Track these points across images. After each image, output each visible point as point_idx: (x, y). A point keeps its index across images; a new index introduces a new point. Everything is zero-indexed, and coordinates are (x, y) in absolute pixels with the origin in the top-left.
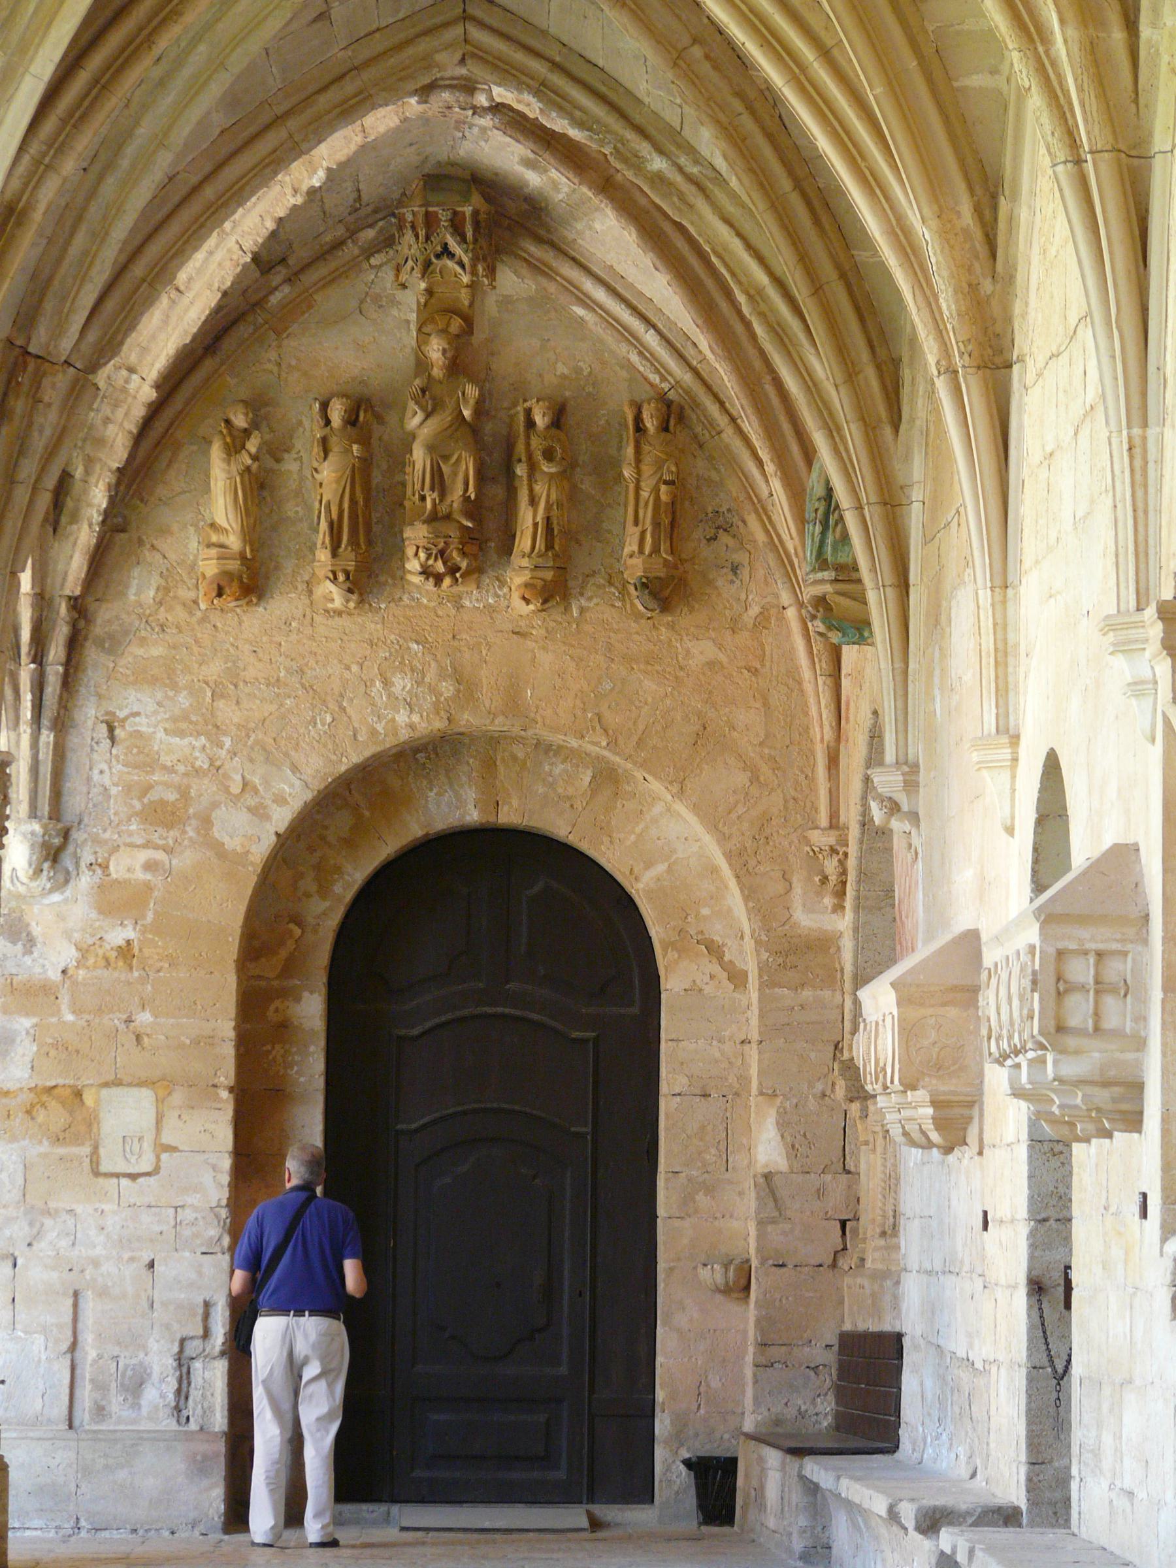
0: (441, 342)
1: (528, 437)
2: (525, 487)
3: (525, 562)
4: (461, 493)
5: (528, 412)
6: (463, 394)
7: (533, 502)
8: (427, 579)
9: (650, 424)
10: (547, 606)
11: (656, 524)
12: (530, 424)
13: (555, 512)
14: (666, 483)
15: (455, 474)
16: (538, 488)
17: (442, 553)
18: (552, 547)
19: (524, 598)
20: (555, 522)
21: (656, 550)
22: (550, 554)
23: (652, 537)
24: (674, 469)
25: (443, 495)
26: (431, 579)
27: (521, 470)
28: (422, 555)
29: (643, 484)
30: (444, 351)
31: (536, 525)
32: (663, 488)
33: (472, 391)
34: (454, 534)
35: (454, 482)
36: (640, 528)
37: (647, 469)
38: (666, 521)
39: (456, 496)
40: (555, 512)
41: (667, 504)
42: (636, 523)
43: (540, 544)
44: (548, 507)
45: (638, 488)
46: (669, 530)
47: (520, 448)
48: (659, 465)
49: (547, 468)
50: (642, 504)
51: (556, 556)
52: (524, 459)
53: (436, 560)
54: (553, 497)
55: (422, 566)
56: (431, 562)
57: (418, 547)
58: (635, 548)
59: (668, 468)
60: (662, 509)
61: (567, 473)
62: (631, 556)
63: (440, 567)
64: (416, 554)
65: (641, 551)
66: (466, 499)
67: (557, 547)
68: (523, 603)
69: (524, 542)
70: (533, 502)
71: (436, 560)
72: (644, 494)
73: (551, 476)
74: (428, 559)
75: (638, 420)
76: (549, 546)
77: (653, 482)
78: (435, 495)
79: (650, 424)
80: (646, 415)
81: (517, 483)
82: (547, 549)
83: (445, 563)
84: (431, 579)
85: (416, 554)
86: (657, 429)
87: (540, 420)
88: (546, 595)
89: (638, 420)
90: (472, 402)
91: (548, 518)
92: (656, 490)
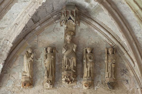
3: (85, 79)
5: (86, 50)
7: (87, 67)
9: (110, 52)
10: (90, 87)
11: (111, 71)
12: (87, 52)
13: (91, 69)
14: (113, 63)
16: (88, 64)
18: (91, 76)
19: (85, 86)
20: (91, 71)
21: (111, 77)
22: (90, 77)
23: (111, 74)
24: (115, 61)
27: (85, 61)
29: (109, 64)
31: (88, 71)
32: (113, 64)
36: (108, 72)
37: (109, 61)
38: (113, 71)
40: (91, 69)
41: (114, 68)
42: (107, 71)
43: (89, 75)
44: (90, 68)
45: (108, 64)
46: (114, 73)
47: (85, 57)
48: (112, 60)
49: (90, 60)
50: (109, 67)
51: (92, 78)
54: (91, 66)
58: (107, 76)
59: (114, 61)
60: (113, 68)
61: (94, 61)
62: (106, 78)
65: (109, 77)
67: (92, 76)
68: (85, 87)
69: (85, 75)
70: (87, 67)
72: (109, 66)
73: (91, 62)
75: (108, 51)
76: (90, 76)
77: (111, 63)
79: (110, 52)
80: (109, 50)
81: (84, 64)
82: (90, 76)
86: (111, 53)
87: (89, 51)
88: (90, 85)
89: (108, 51)
91: (90, 70)
92: (111, 65)
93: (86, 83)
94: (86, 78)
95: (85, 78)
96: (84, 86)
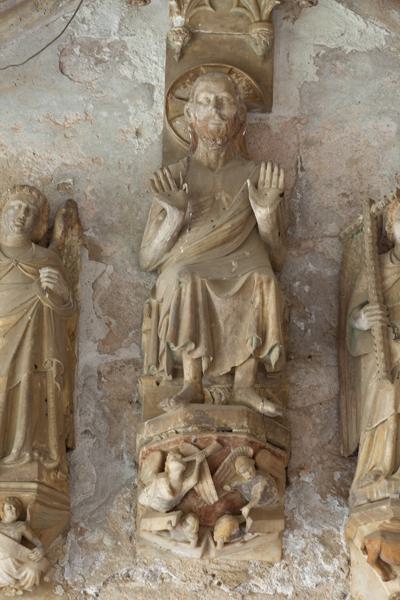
0: (213, 86)
1: (380, 266)
2: (379, 347)
3: (380, 489)
4: (251, 350)
6: (256, 186)
8: (181, 521)
15: (240, 316)
17: (213, 465)
19: (379, 563)
25: (214, 352)
26: (191, 522)
28: (174, 467)
30: (218, 104)
33: (271, 179)
34: (240, 431)
35: (236, 331)
39: (239, 355)
47: (366, 284)
52: (373, 296)
53: (200, 478)
55: (173, 491)
56: (190, 483)
57: (164, 455)
63: (208, 490)
64: (162, 468)
66: (261, 367)
68: (377, 574)
71: (200, 478)
74: (184, 475)
78: (200, 352)
81: (360, 348)
83: (218, 487)
84: (191, 522)
85: (162, 468)
90: (271, 193)
93: (384, 533)
94: (384, 482)
95: (377, 477)
96: (361, 561)
